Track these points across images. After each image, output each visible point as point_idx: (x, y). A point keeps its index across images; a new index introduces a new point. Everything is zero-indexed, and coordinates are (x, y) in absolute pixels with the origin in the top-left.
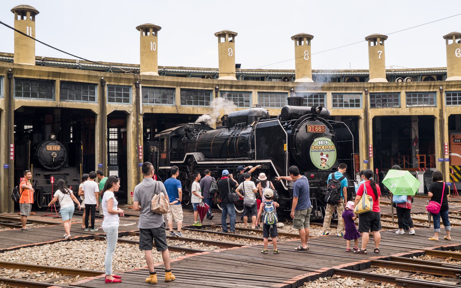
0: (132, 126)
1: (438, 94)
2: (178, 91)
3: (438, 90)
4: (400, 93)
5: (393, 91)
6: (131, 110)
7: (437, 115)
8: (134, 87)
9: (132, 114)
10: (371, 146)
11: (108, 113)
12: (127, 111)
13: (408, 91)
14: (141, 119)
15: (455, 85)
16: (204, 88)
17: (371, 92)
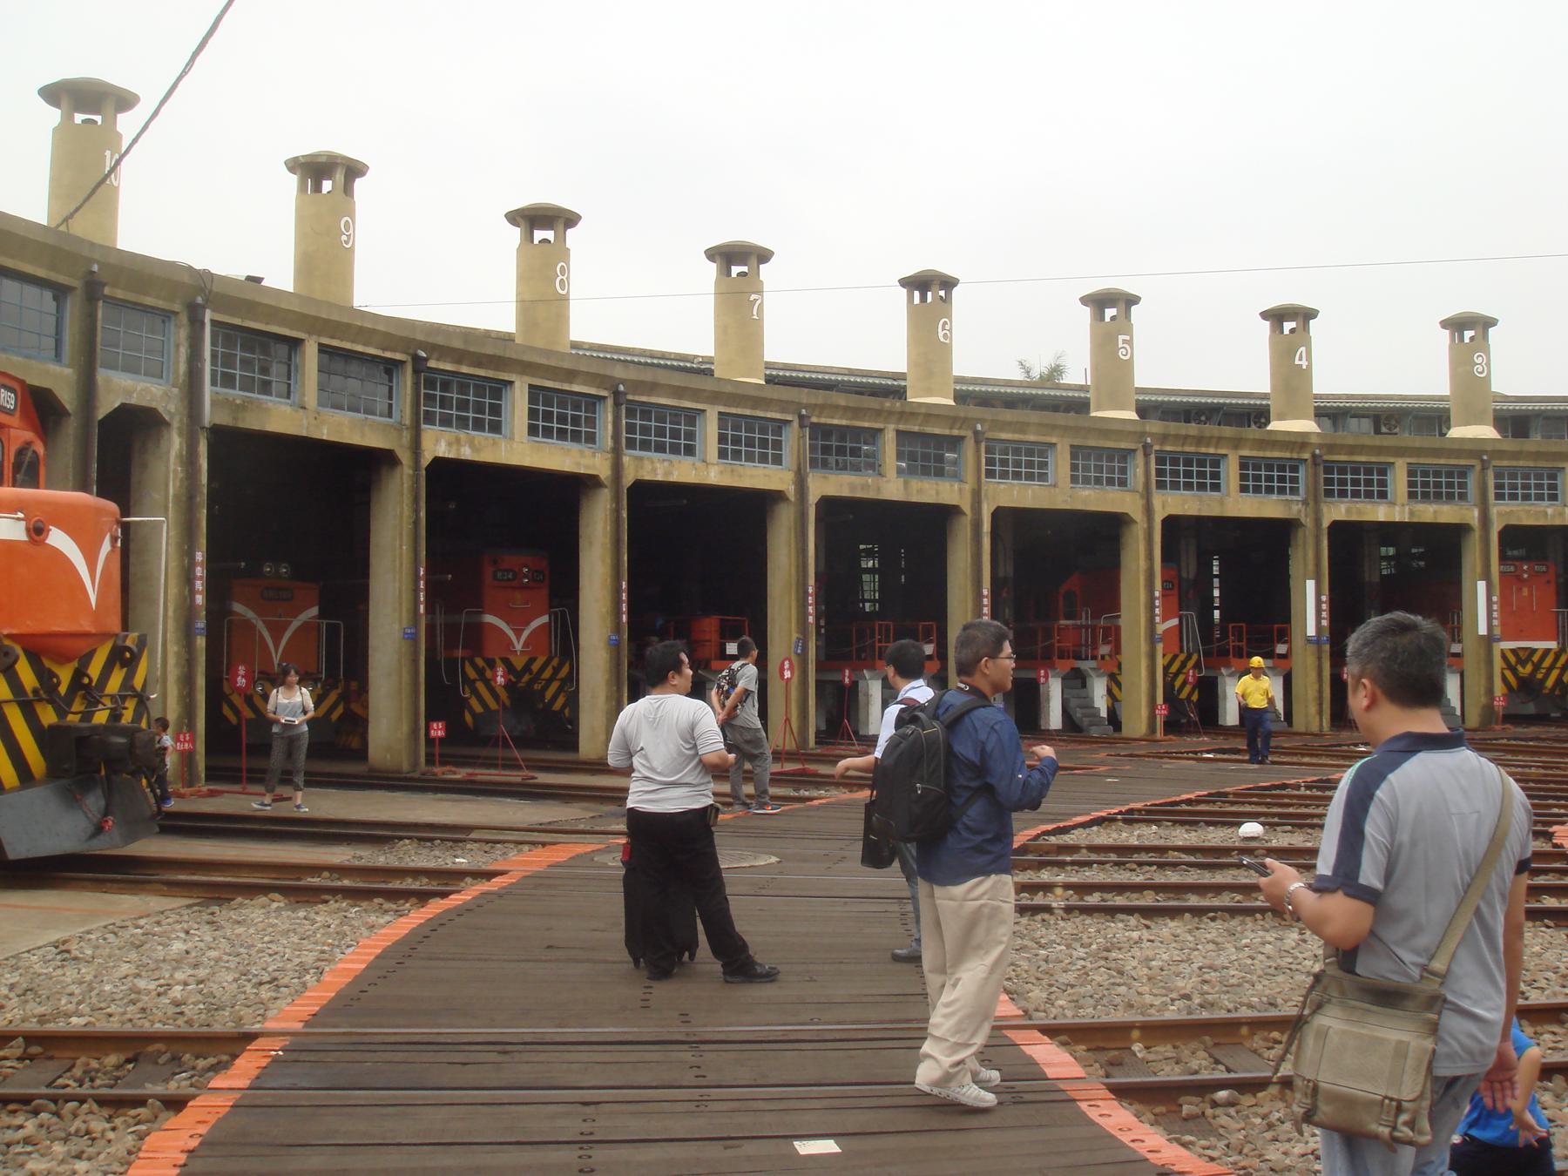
0: (175, 471)
1: (969, 445)
2: (311, 352)
3: (969, 434)
4: (881, 430)
5: (866, 425)
6: (172, 407)
7: (966, 507)
8: (184, 318)
9: (175, 424)
10: (810, 590)
11: (101, 413)
12: (161, 410)
13: (902, 427)
14: (203, 448)
15: (1010, 423)
16: (384, 350)
17: (814, 420)
